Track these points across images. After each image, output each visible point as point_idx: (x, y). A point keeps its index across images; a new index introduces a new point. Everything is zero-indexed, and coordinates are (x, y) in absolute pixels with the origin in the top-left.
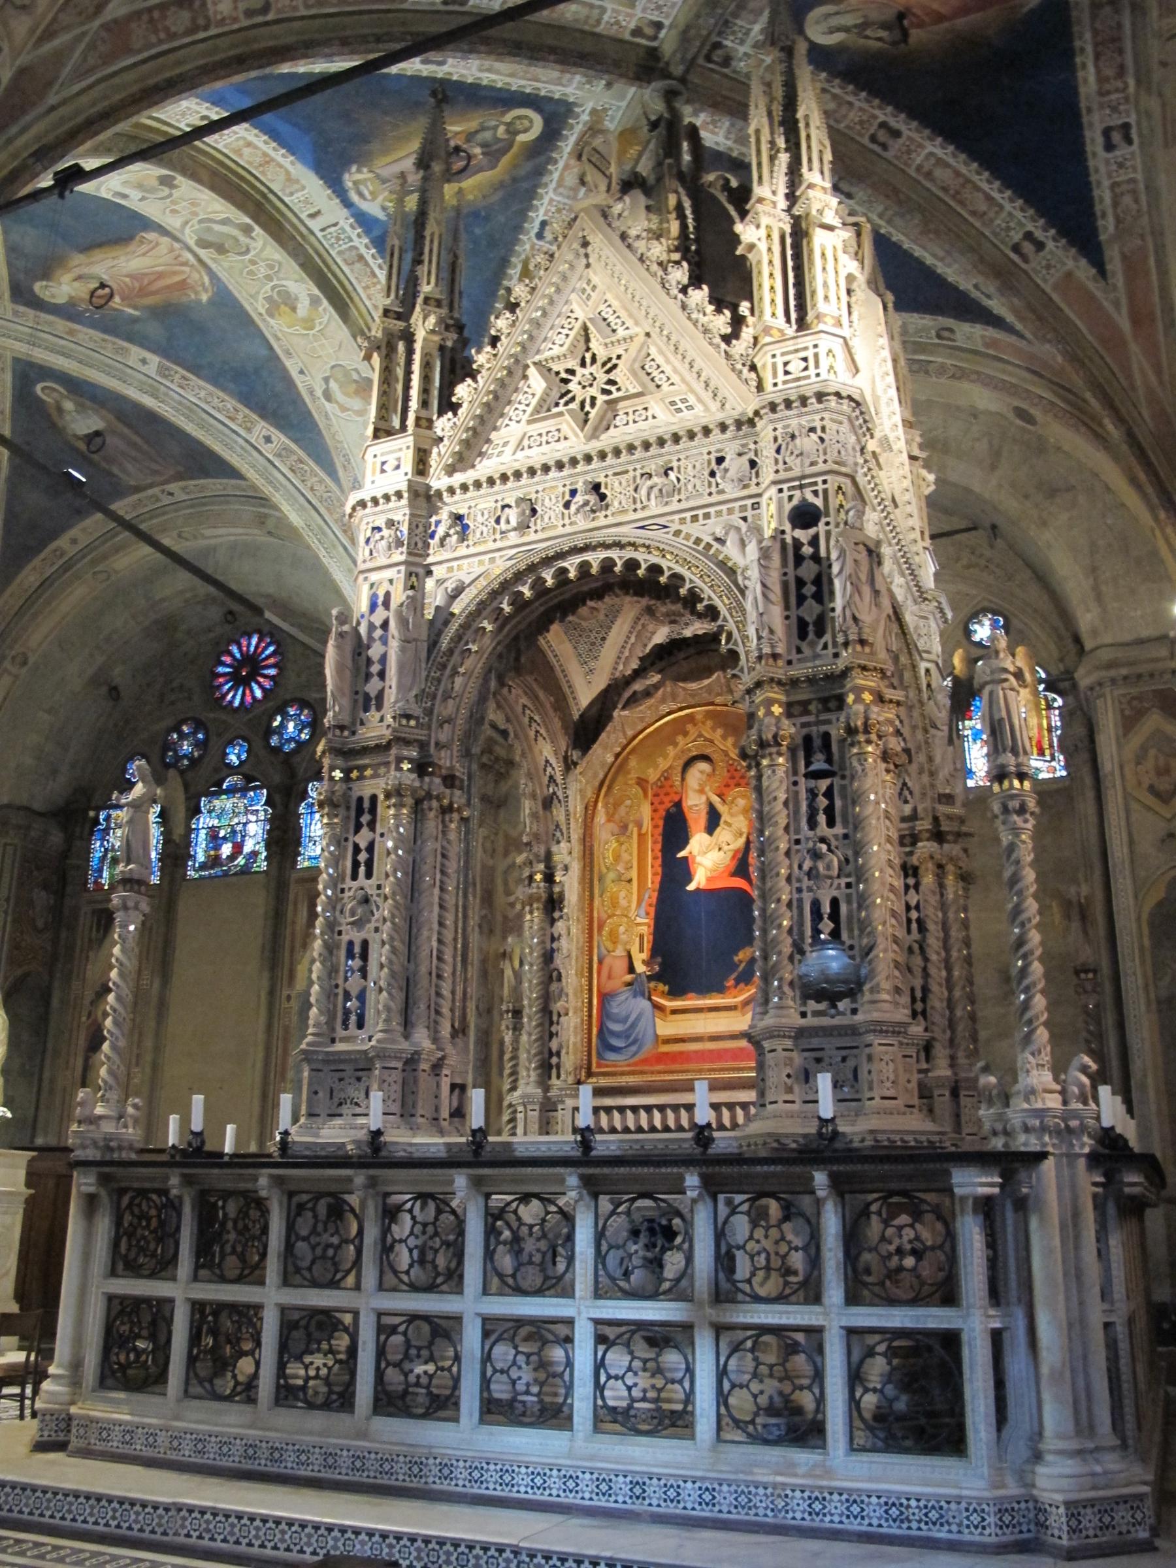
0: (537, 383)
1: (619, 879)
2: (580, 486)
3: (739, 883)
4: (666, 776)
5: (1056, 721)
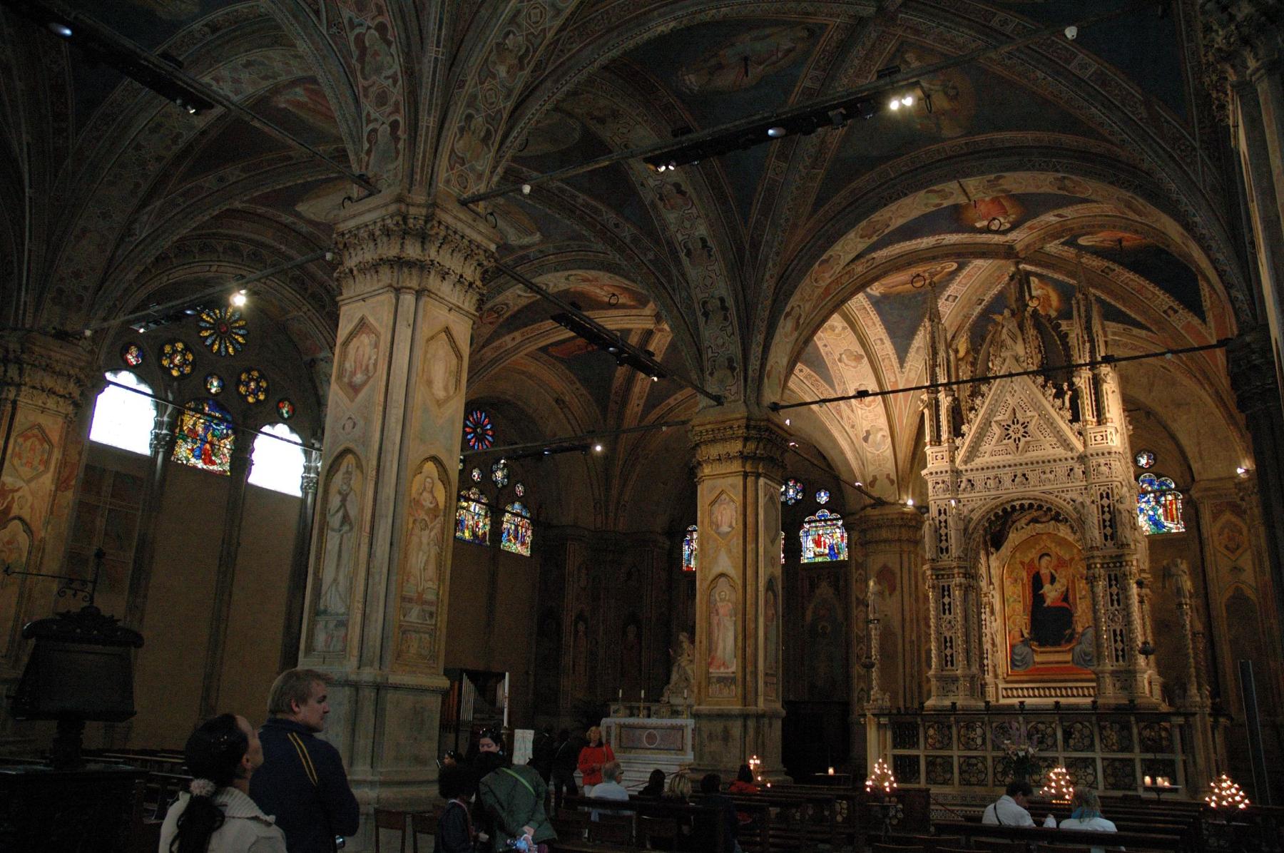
0: (996, 430)
1: (1015, 601)
2: (1019, 474)
3: (1065, 605)
4: (1032, 560)
5: (1180, 506)
